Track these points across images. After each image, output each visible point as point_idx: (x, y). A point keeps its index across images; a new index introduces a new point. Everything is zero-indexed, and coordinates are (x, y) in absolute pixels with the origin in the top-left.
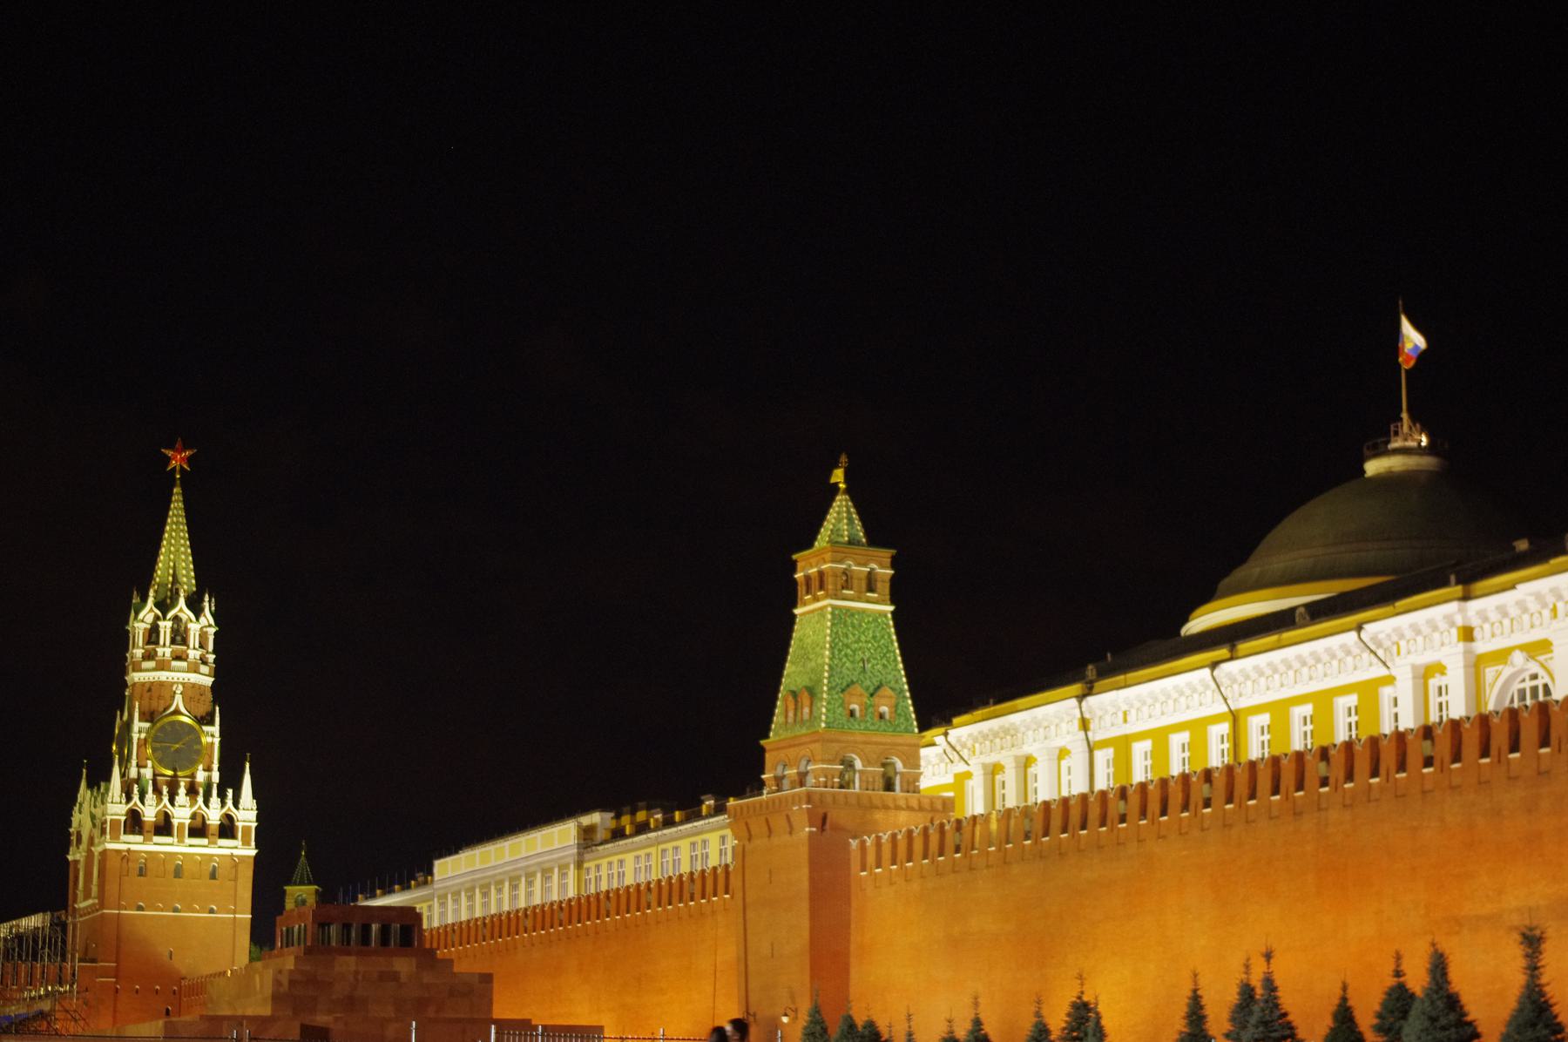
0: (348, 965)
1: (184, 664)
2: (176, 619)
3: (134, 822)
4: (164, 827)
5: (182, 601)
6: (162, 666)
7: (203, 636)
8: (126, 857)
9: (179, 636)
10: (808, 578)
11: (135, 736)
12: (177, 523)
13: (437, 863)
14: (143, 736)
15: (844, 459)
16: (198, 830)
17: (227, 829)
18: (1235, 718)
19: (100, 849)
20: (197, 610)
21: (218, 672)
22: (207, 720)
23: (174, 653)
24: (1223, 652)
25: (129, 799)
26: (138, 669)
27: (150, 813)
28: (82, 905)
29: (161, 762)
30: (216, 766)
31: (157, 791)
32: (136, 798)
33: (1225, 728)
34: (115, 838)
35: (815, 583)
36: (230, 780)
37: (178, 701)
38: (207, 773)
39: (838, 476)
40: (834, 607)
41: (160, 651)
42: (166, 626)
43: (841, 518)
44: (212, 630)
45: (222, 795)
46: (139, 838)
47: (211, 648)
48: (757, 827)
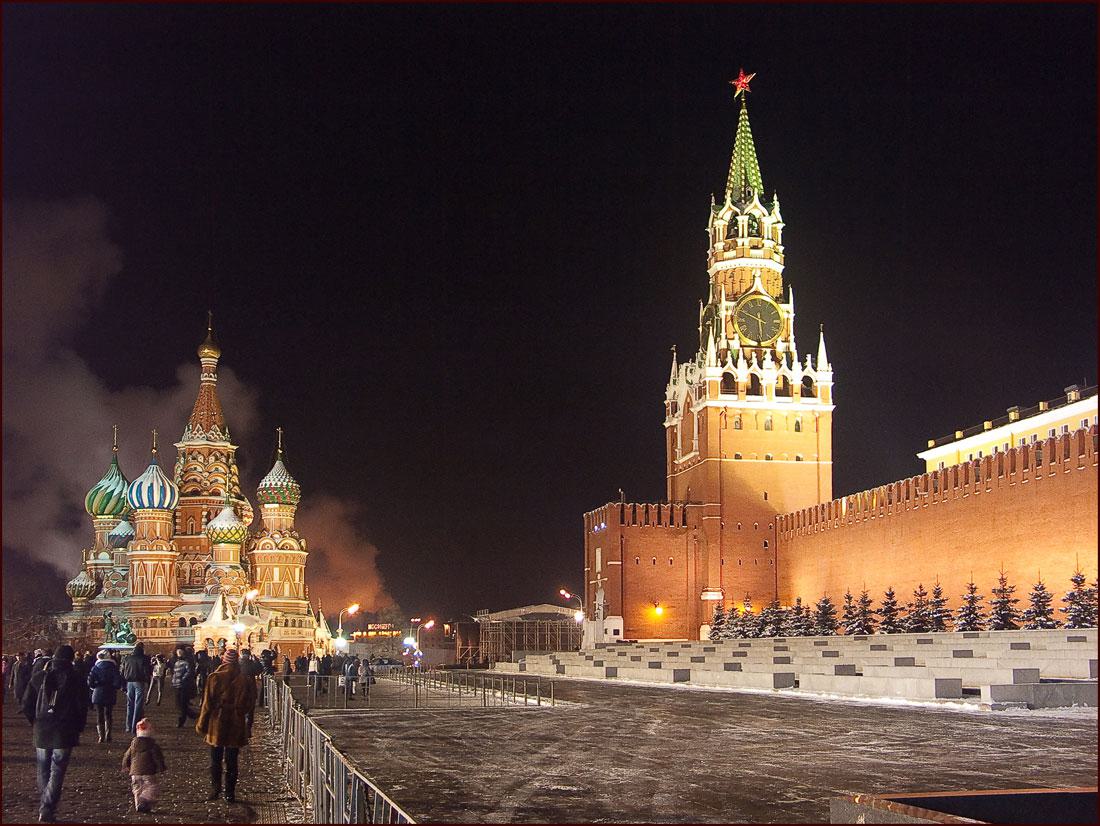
2: (752, 217)
3: (729, 384)
4: (755, 388)
5: (756, 198)
8: (724, 413)
9: (756, 230)
12: (745, 138)
14: (730, 313)
16: (784, 391)
23: (749, 250)
25: (723, 364)
27: (742, 375)
28: (680, 460)
30: (792, 338)
36: (806, 348)
38: (785, 342)
41: (740, 241)
42: (743, 220)
45: (802, 360)
46: (734, 397)
47: (780, 242)
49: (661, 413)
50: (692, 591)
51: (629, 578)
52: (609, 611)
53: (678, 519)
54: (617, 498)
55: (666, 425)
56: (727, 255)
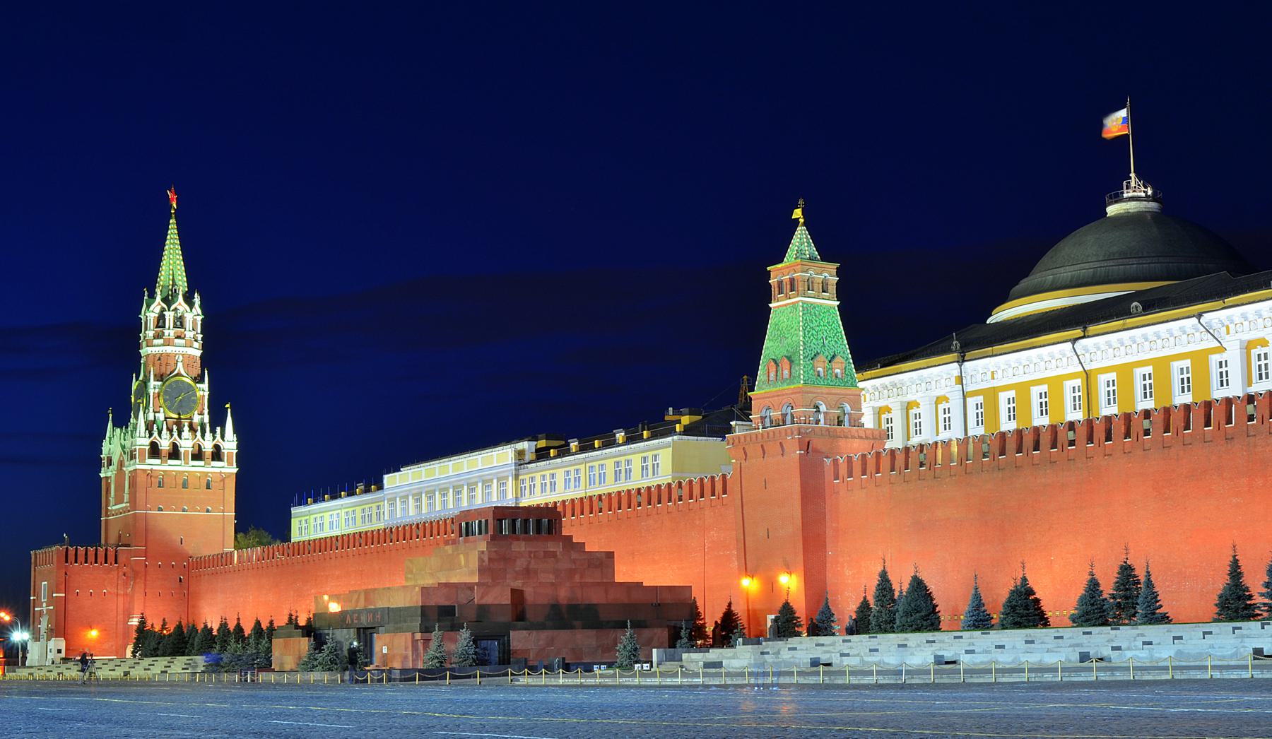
0: (519, 547)
1: (182, 342)
3: (154, 451)
4: (175, 453)
6: (168, 343)
7: (195, 321)
8: (150, 474)
9: (180, 322)
10: (780, 283)
11: (151, 392)
13: (386, 477)
15: (801, 202)
16: (198, 455)
17: (217, 455)
18: (1088, 376)
19: (131, 469)
20: (191, 305)
21: (204, 347)
22: (199, 379)
24: (1078, 332)
25: (151, 435)
27: (165, 444)
28: (113, 508)
29: (169, 409)
30: (206, 411)
31: (170, 430)
32: (156, 434)
33: (1078, 382)
34: (142, 461)
35: (786, 287)
36: (217, 420)
38: (201, 416)
39: (797, 213)
40: (804, 303)
41: (166, 332)
42: (169, 316)
43: (801, 241)
44: (200, 318)
45: (213, 431)
46: (158, 461)
48: (754, 450)
49: (98, 464)
50: (120, 617)
51: (70, 607)
52: (55, 632)
54: (61, 541)
56: (156, 342)
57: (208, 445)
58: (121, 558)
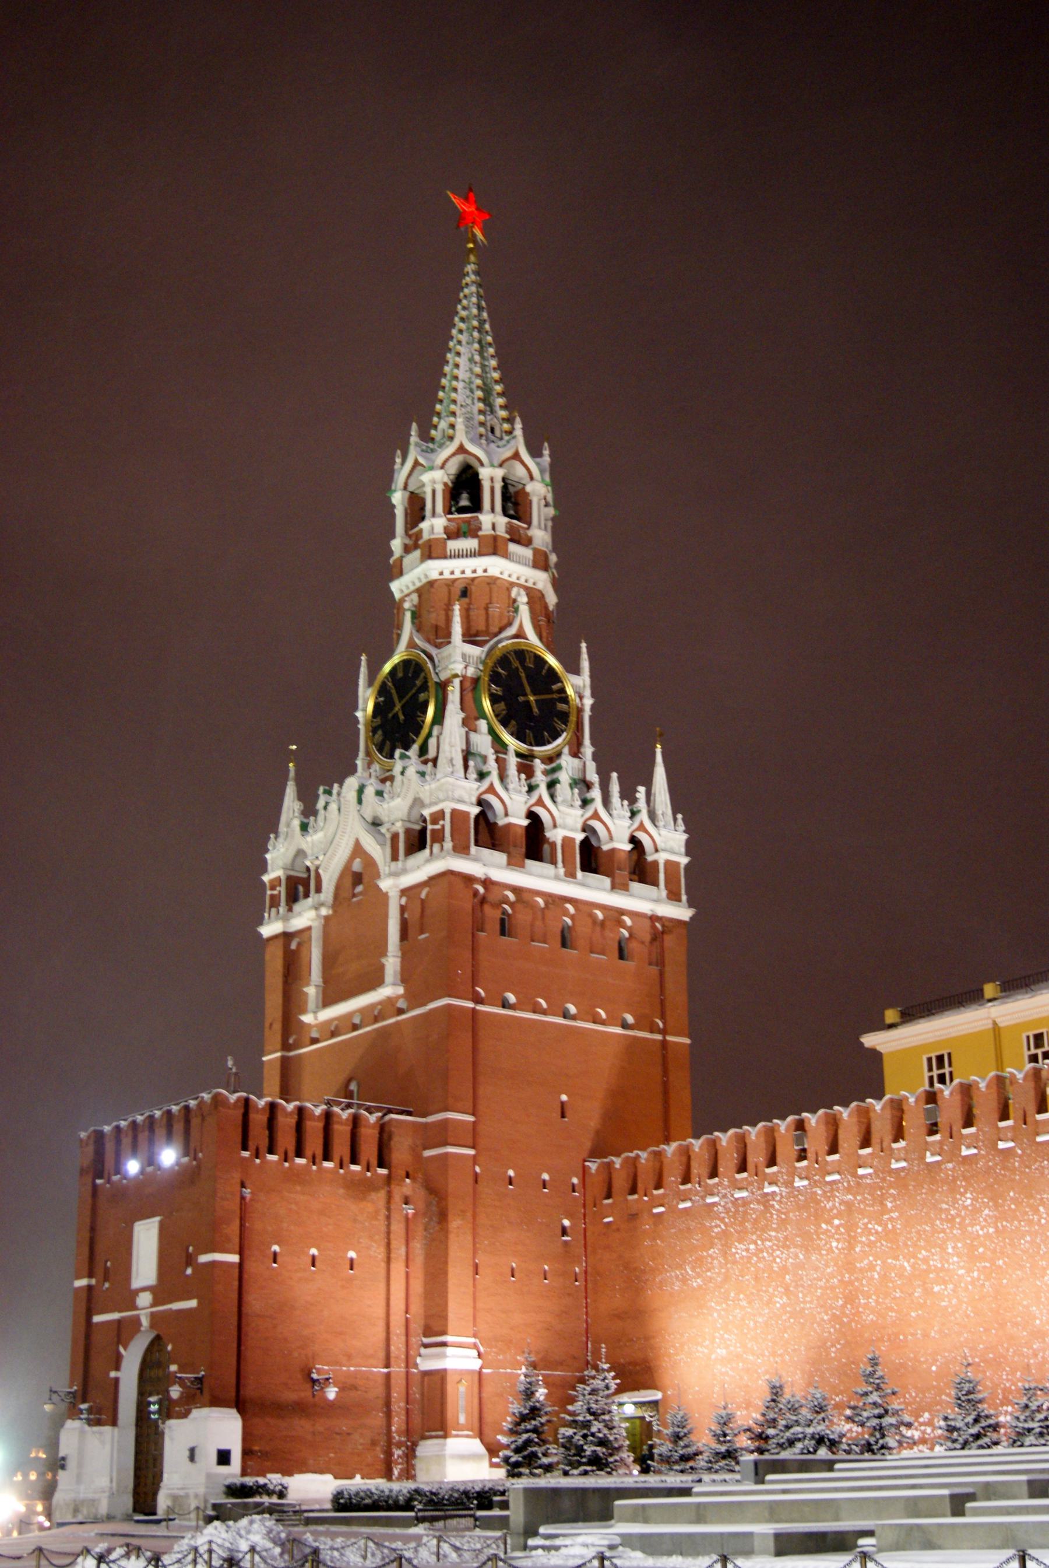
4: (534, 842)
6: (493, 547)
16: (590, 857)
26: (432, 551)
30: (588, 750)
37: (524, 612)
45: (629, 795)
46: (501, 857)
50: (398, 1346)
51: (255, 1302)
53: (369, 1150)
55: (267, 930)
57: (616, 831)
58: (401, 1151)
